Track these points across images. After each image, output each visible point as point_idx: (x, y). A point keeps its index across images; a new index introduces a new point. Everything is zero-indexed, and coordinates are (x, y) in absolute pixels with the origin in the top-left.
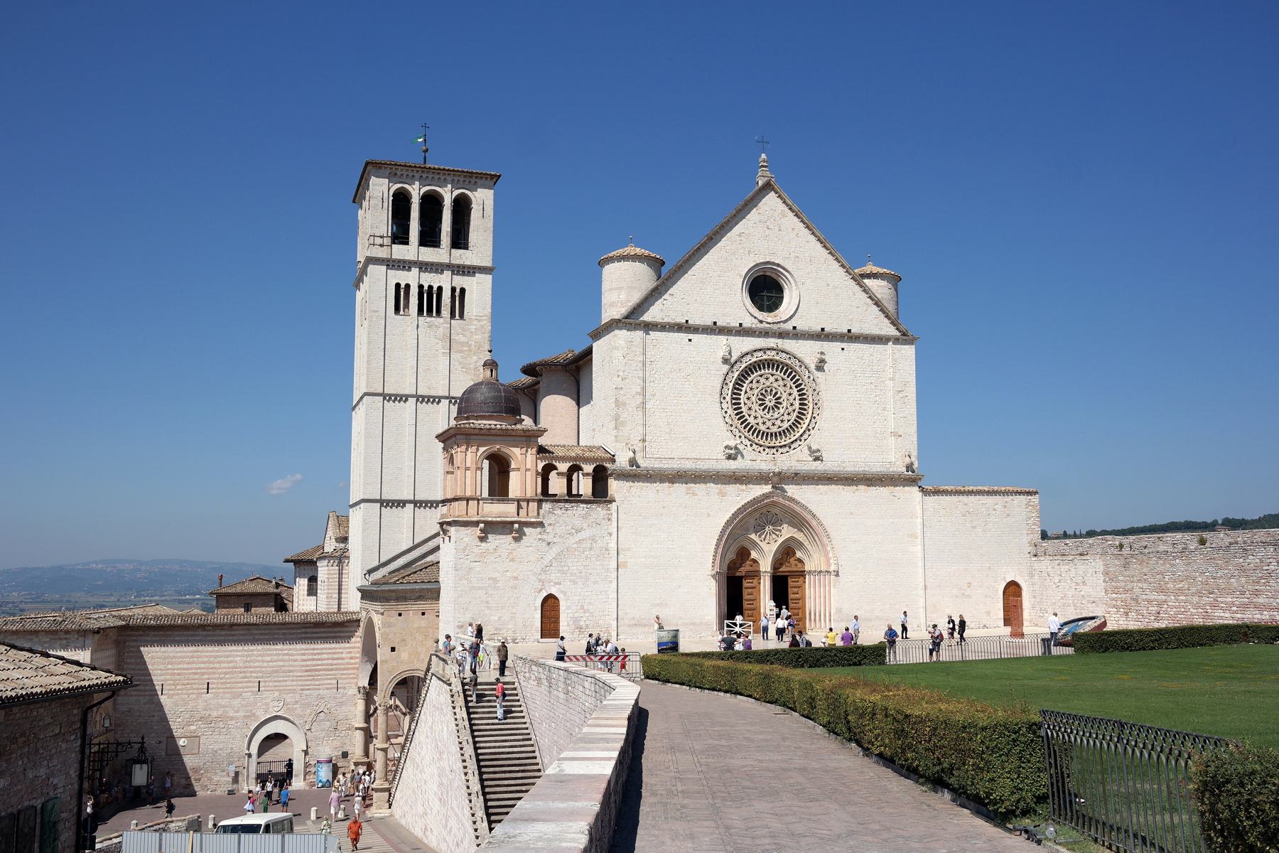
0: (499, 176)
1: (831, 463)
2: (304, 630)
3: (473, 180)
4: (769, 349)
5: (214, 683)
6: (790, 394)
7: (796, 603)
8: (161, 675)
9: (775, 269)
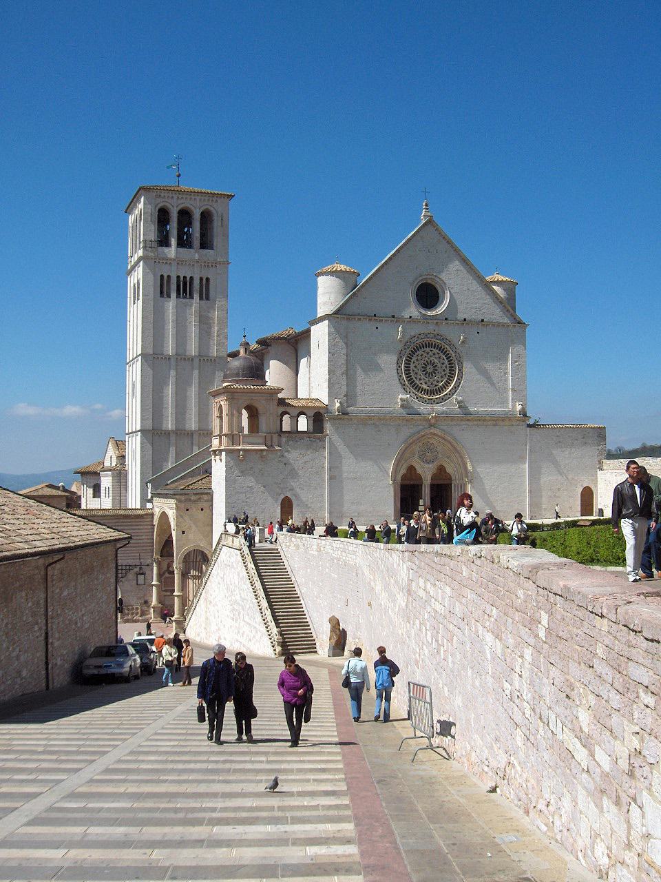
0: (233, 196)
3: (215, 199)
6: (443, 364)
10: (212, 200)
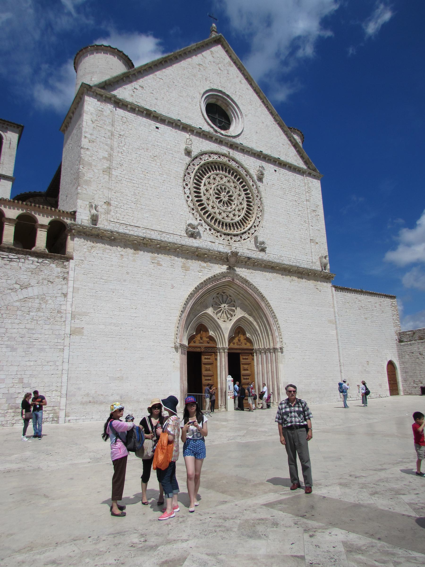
4: (223, 155)
6: (239, 195)
7: (247, 379)
9: (224, 98)
10: (3, 127)
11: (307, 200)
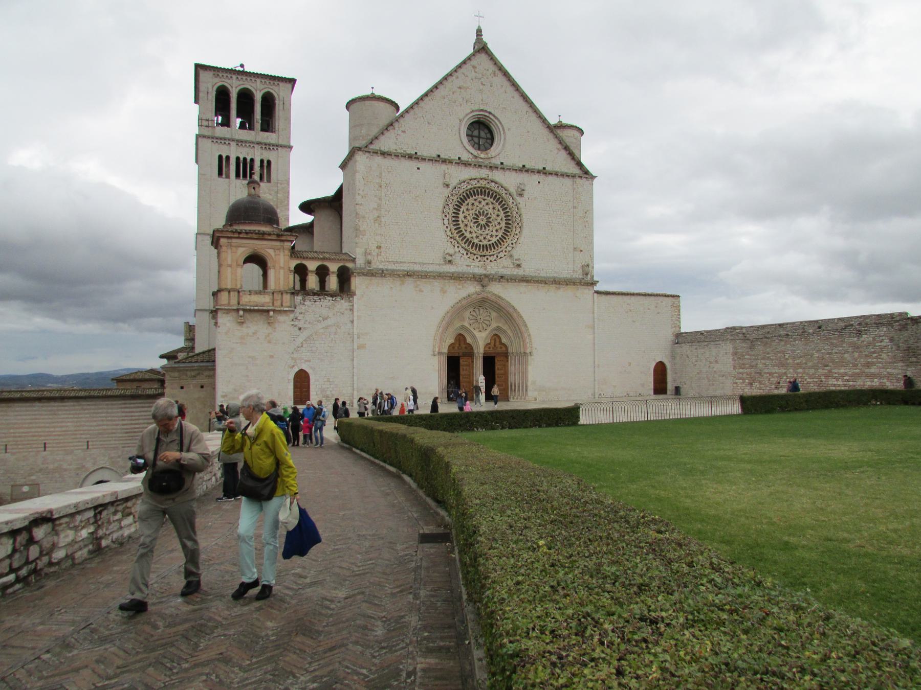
1: (528, 269)
2: (123, 402)
3: (276, 83)
5: (49, 443)
6: (498, 216)
8: (5, 437)
11: (575, 207)
